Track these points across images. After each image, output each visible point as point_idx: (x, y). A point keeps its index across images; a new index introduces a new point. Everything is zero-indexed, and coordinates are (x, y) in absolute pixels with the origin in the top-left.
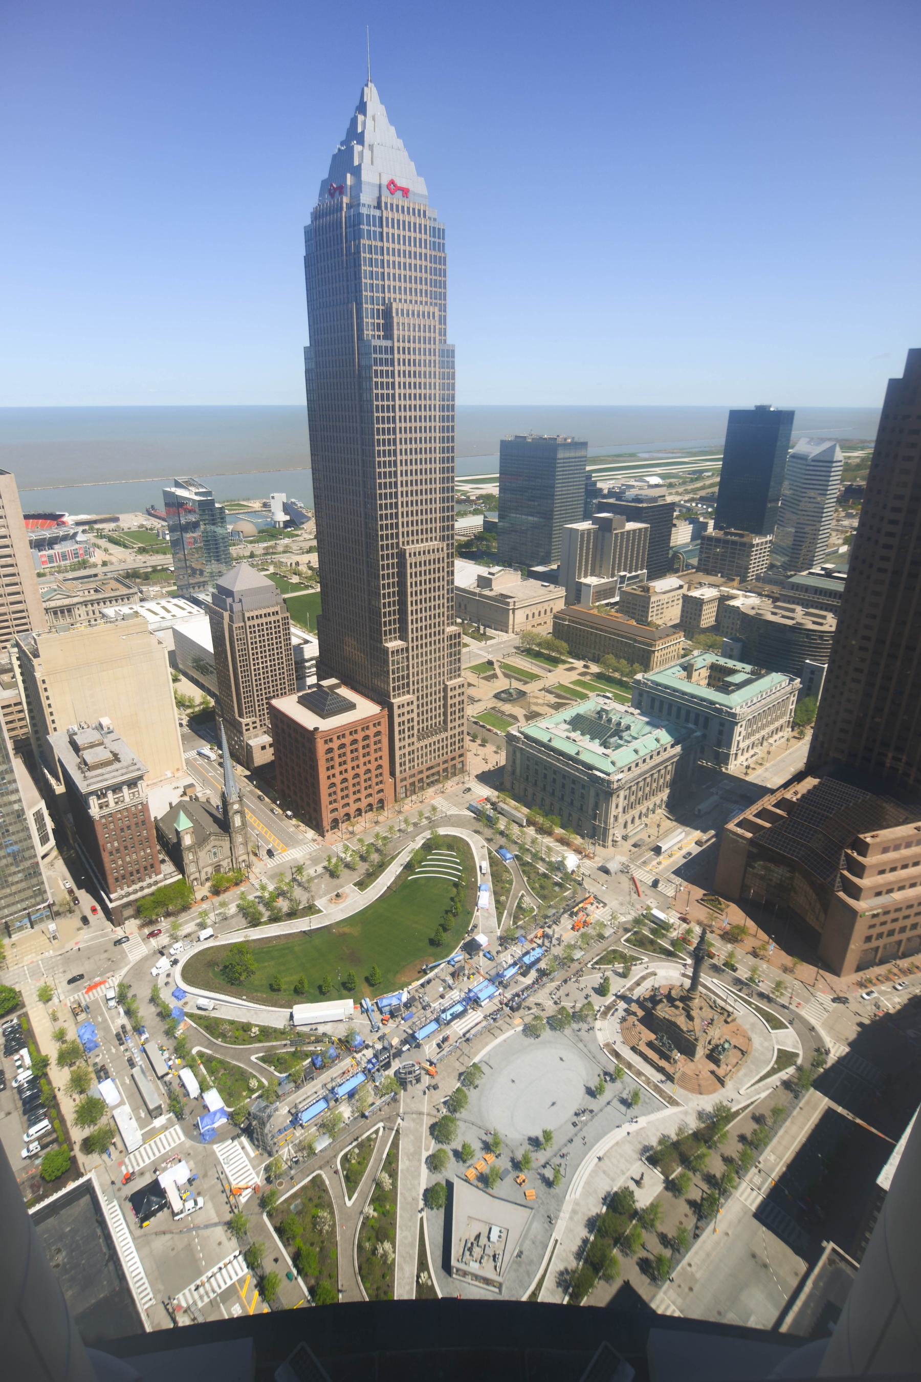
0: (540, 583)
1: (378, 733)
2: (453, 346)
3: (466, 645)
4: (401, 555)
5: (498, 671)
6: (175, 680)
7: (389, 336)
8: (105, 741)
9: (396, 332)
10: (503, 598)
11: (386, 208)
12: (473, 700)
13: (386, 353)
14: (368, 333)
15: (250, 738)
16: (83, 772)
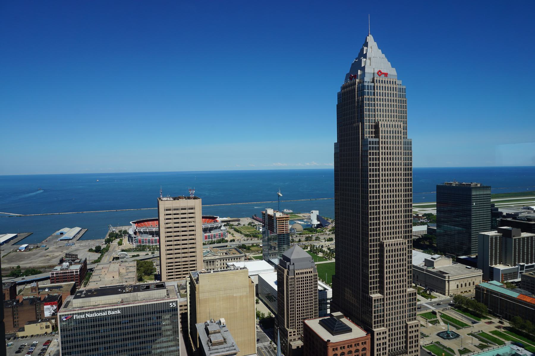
0: (465, 266)
1: (364, 349)
2: (411, 139)
3: (419, 300)
4: (381, 245)
5: (439, 318)
6: (257, 303)
7: (377, 136)
8: (221, 331)
9: (381, 135)
10: (442, 273)
11: (377, 82)
12: (424, 336)
13: (376, 144)
14: (367, 136)
15: (291, 340)
16: (209, 346)
